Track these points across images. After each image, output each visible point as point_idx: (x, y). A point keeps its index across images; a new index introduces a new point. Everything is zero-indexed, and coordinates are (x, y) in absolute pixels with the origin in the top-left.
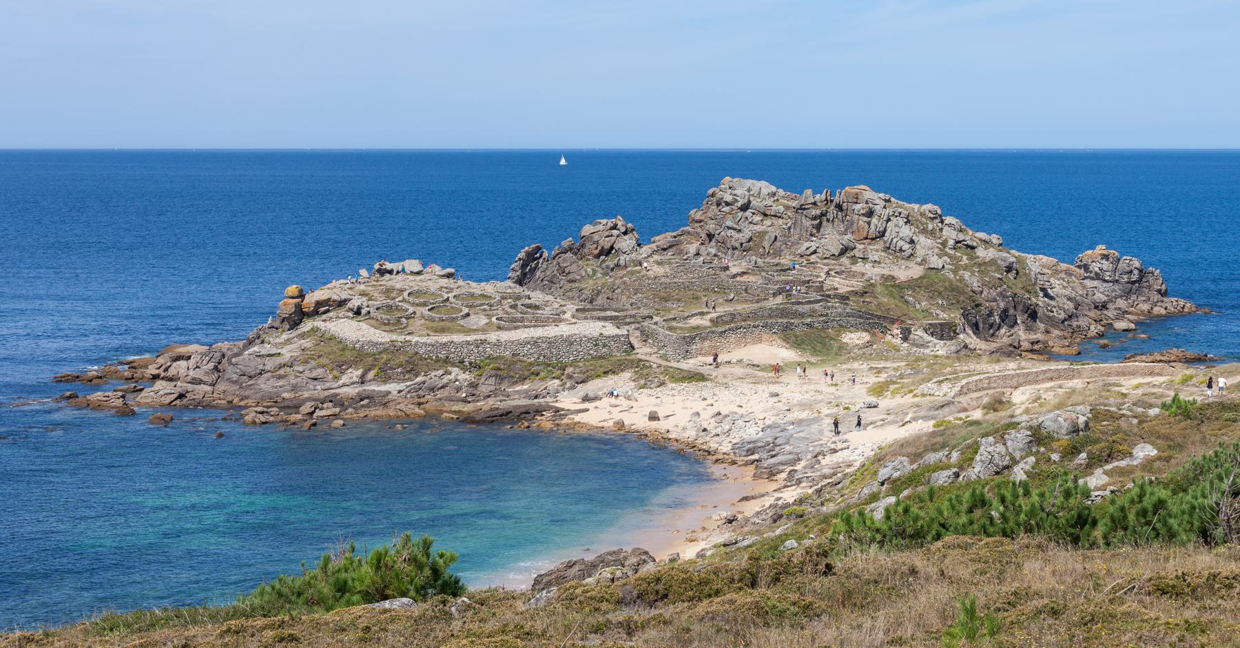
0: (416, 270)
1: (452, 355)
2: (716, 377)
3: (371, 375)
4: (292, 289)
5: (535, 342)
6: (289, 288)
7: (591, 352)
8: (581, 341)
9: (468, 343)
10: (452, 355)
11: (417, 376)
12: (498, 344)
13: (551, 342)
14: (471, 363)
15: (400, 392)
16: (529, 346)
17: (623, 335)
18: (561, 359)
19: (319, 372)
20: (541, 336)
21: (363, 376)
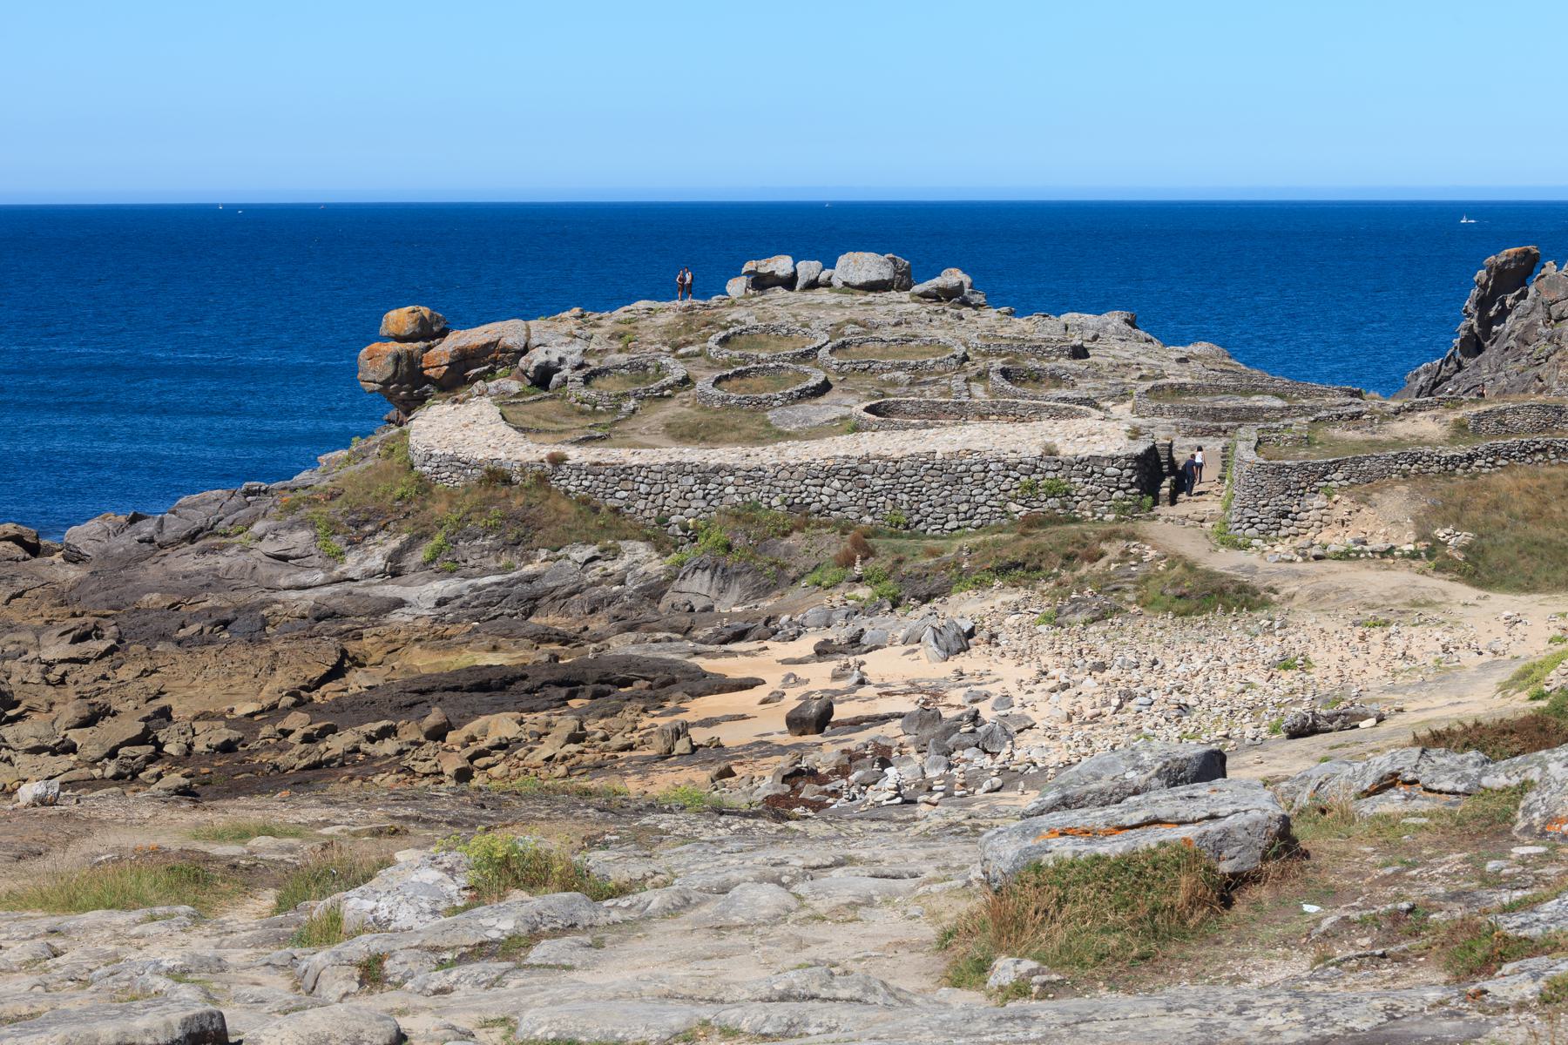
0: (860, 278)
1: (641, 504)
2: (1291, 597)
3: (421, 554)
4: (400, 318)
5: (854, 473)
6: (393, 314)
7: (1013, 507)
8: (986, 471)
9: (682, 469)
10: (641, 504)
11: (529, 560)
12: (754, 476)
13: (894, 470)
14: (685, 529)
15: (441, 603)
16: (836, 484)
17: (1113, 459)
18: (922, 526)
19: (300, 539)
20: (872, 453)
21: (396, 557)
